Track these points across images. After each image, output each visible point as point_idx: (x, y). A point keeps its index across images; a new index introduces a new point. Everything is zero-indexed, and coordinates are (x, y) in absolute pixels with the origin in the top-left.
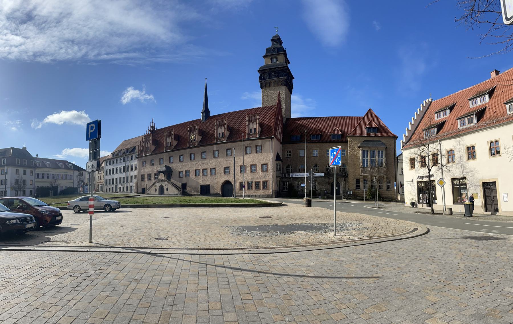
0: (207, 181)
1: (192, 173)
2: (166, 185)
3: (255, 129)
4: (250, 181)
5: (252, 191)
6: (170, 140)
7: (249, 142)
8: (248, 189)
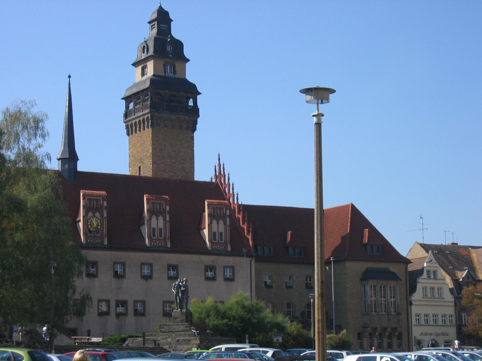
7: (212, 258)
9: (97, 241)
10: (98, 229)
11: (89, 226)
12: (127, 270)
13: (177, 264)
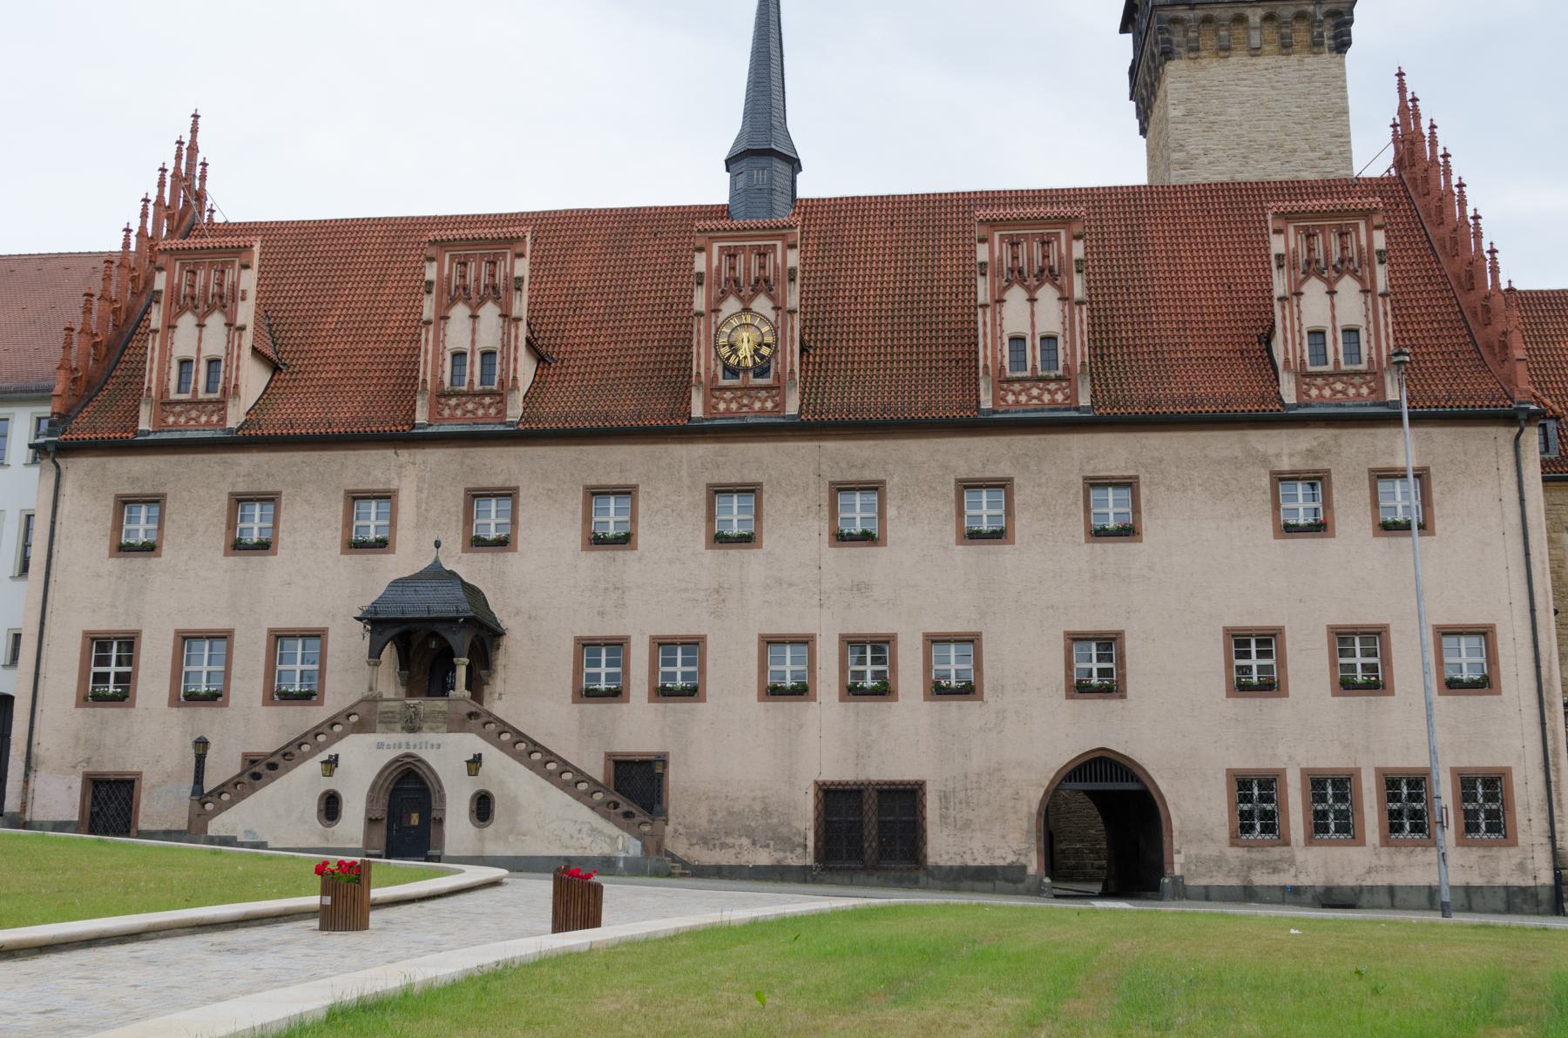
0: (901, 742)
1: (732, 669)
2: (475, 763)
3: (1351, 332)
4: (1330, 760)
5: (1353, 852)
6: (470, 330)
8: (1318, 826)
9: (757, 405)
10: (762, 357)
11: (725, 351)
12: (891, 512)
13: (1132, 473)
